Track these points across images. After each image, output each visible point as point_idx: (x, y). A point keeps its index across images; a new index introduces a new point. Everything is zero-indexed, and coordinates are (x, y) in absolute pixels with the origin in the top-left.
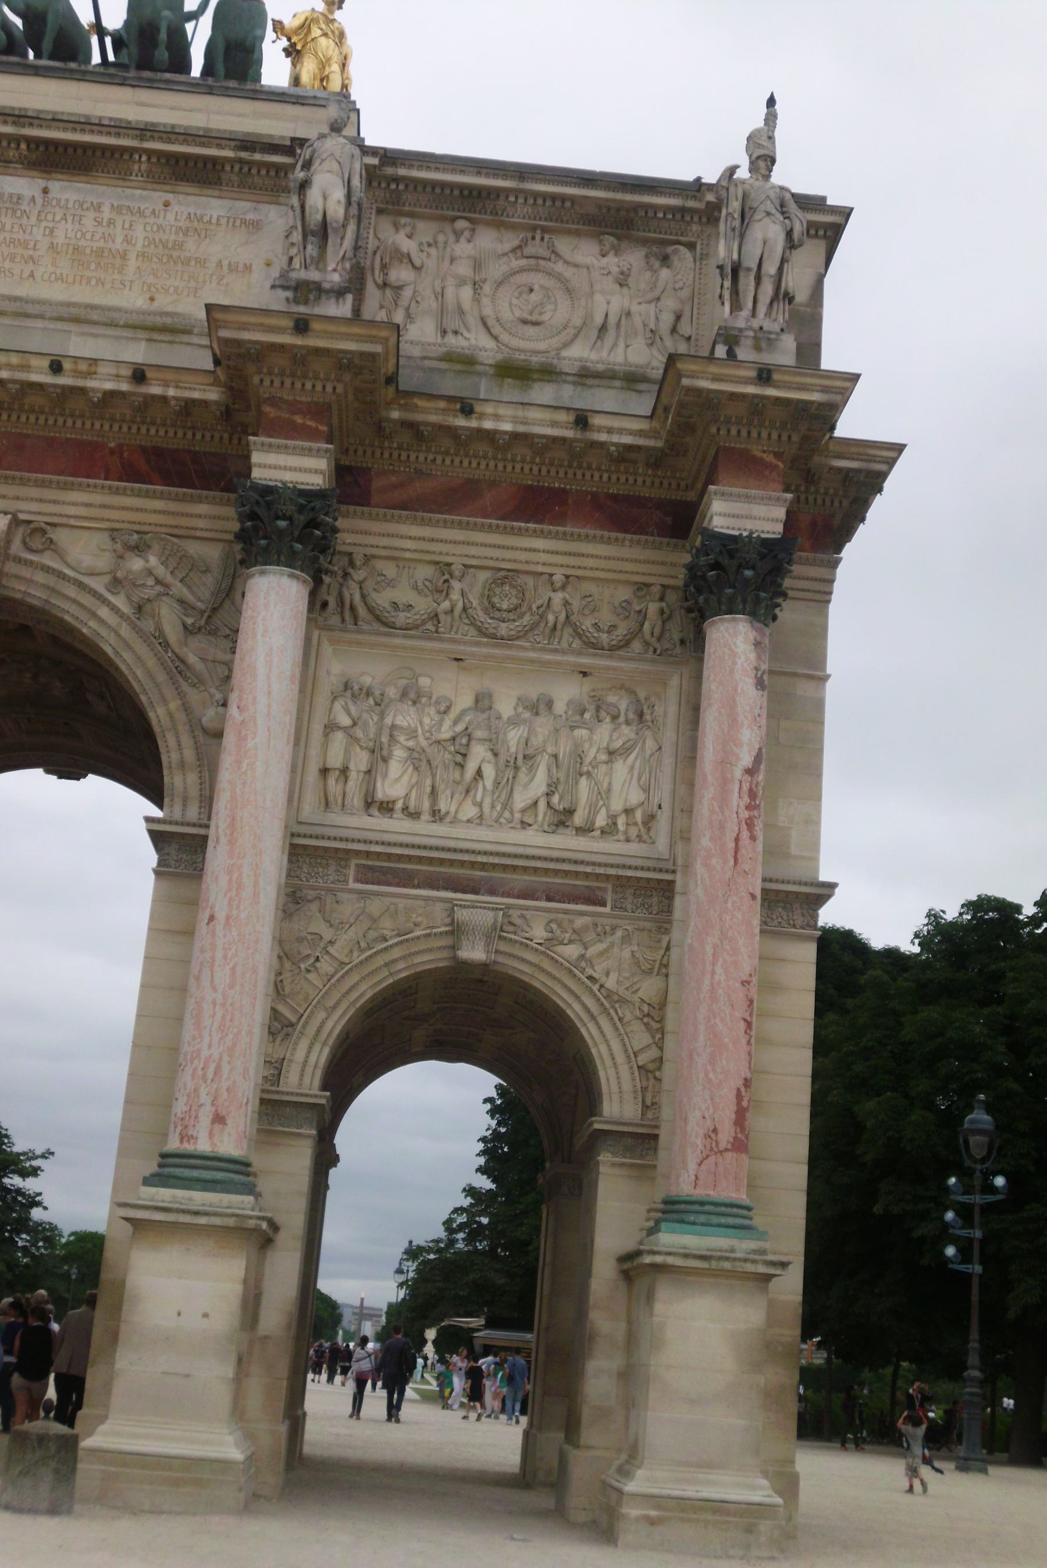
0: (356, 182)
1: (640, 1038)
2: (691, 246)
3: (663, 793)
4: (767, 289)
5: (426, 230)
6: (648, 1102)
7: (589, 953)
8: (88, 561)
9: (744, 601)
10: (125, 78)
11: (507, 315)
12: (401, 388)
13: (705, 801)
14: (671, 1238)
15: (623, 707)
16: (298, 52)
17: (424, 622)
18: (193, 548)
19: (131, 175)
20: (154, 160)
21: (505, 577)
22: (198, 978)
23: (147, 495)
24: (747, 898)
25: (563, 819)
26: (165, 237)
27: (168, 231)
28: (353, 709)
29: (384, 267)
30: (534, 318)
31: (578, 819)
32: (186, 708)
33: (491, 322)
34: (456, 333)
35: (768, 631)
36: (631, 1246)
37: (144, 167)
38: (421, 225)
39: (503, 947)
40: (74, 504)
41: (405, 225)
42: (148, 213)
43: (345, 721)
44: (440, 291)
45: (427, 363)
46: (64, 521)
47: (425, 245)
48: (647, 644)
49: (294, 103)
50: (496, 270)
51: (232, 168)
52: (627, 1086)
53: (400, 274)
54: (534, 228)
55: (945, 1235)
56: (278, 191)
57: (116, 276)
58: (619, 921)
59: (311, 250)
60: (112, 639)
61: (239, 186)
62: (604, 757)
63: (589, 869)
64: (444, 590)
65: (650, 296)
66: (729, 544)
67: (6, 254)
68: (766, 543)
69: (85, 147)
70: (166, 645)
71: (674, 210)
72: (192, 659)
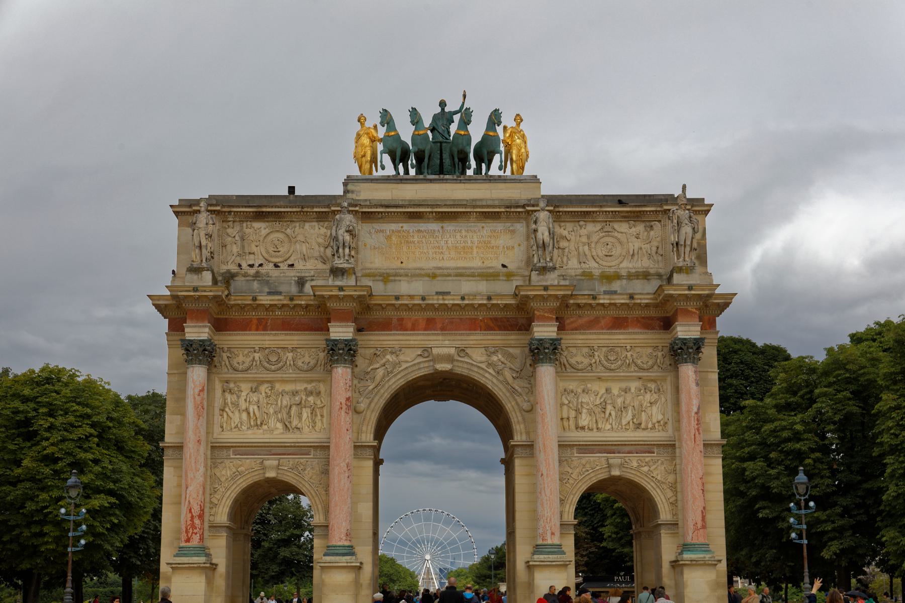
1: (670, 494)
2: (660, 221)
3: (669, 415)
4: (688, 249)
5: (569, 226)
6: (674, 513)
7: (651, 469)
8: (479, 359)
9: (690, 359)
11: (600, 254)
13: (684, 424)
14: (687, 556)
15: (653, 387)
17: (587, 367)
18: (511, 350)
20: (478, 214)
21: (612, 349)
22: (540, 493)
23: (495, 335)
24: (699, 453)
25: (638, 426)
28: (569, 398)
29: (558, 242)
30: (610, 254)
31: (643, 426)
32: (517, 404)
33: (595, 257)
34: (584, 263)
35: (698, 366)
36: (673, 559)
38: (568, 224)
39: (624, 470)
40: (472, 340)
43: (567, 402)
45: (578, 277)
46: (470, 346)
48: (659, 366)
50: (595, 238)
52: (667, 509)
53: (563, 244)
54: (606, 221)
55: (790, 528)
58: (659, 458)
60: (490, 383)
62: (649, 405)
63: (649, 443)
64: (593, 356)
65: (647, 242)
66: (684, 341)
68: (695, 339)
69: (455, 212)
70: (508, 384)
71: (653, 211)
72: (517, 388)
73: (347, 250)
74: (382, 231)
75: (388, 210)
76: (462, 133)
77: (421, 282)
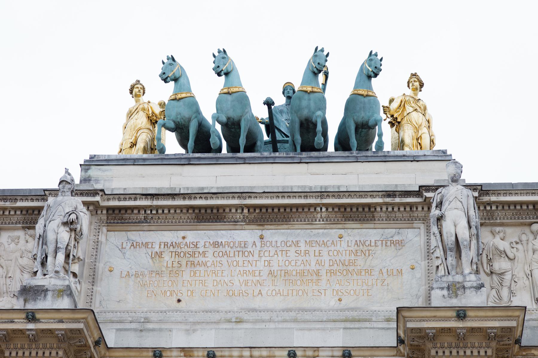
0: (472, 212)
5: (512, 233)
10: (301, 158)
12: (522, 345)
16: (399, 123)
19: (316, 221)
20: (330, 210)
26: (342, 259)
27: (344, 254)
29: (490, 261)
37: (324, 215)
38: (509, 230)
41: (499, 232)
42: (329, 243)
44: (530, 274)
47: (514, 243)
49: (412, 161)
51: (381, 209)
53: (501, 264)
56: (412, 220)
57: (315, 287)
59: (451, 260)
61: (386, 220)
67: (241, 281)
69: (285, 206)
73: (61, 257)
74: (146, 245)
75: (156, 203)
76: (309, 89)
77: (213, 332)
